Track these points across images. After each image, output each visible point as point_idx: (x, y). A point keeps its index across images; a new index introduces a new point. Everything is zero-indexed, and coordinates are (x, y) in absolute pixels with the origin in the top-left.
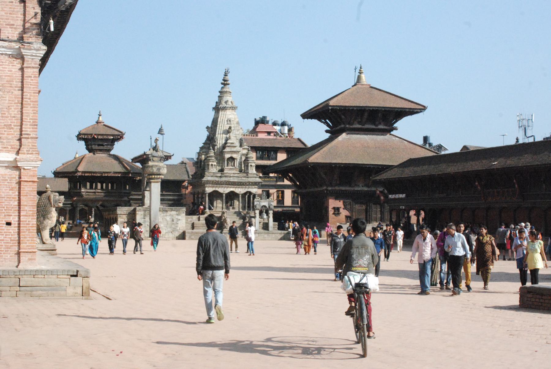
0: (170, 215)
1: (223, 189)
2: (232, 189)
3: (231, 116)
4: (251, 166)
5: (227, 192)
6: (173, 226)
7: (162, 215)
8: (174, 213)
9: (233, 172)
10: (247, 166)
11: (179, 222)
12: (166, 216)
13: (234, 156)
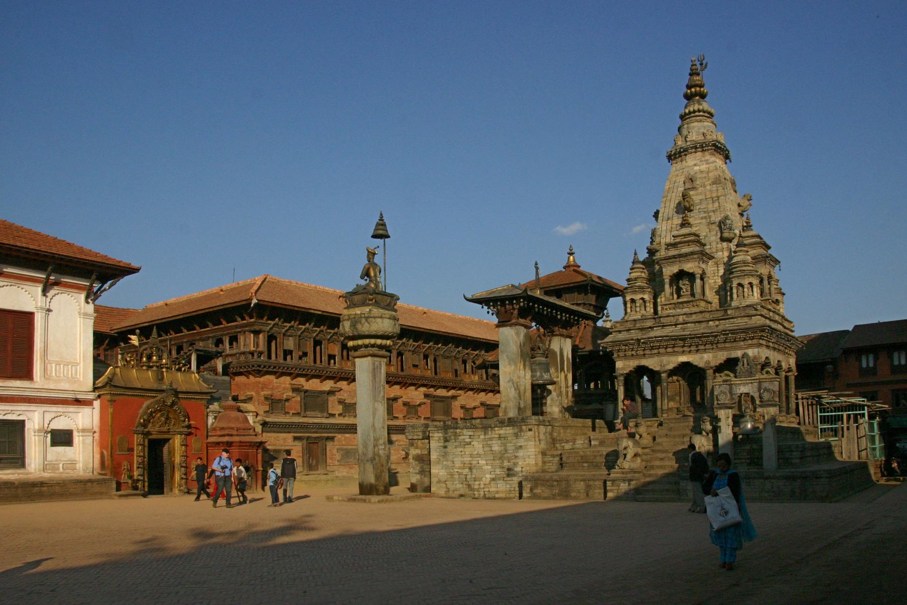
0: (500, 438)
1: (656, 359)
2: (683, 359)
3: (696, 168)
4: (740, 285)
5: (671, 367)
6: (506, 464)
7: (482, 437)
8: (508, 431)
9: (686, 310)
10: (731, 289)
11: (521, 453)
12: (491, 439)
13: (689, 267)
